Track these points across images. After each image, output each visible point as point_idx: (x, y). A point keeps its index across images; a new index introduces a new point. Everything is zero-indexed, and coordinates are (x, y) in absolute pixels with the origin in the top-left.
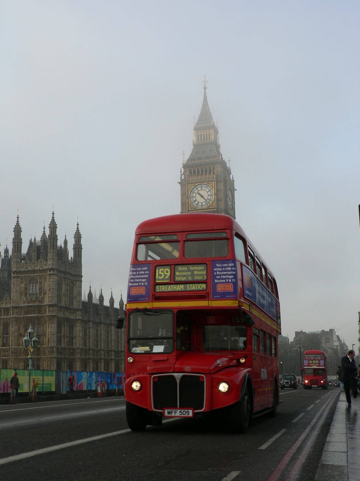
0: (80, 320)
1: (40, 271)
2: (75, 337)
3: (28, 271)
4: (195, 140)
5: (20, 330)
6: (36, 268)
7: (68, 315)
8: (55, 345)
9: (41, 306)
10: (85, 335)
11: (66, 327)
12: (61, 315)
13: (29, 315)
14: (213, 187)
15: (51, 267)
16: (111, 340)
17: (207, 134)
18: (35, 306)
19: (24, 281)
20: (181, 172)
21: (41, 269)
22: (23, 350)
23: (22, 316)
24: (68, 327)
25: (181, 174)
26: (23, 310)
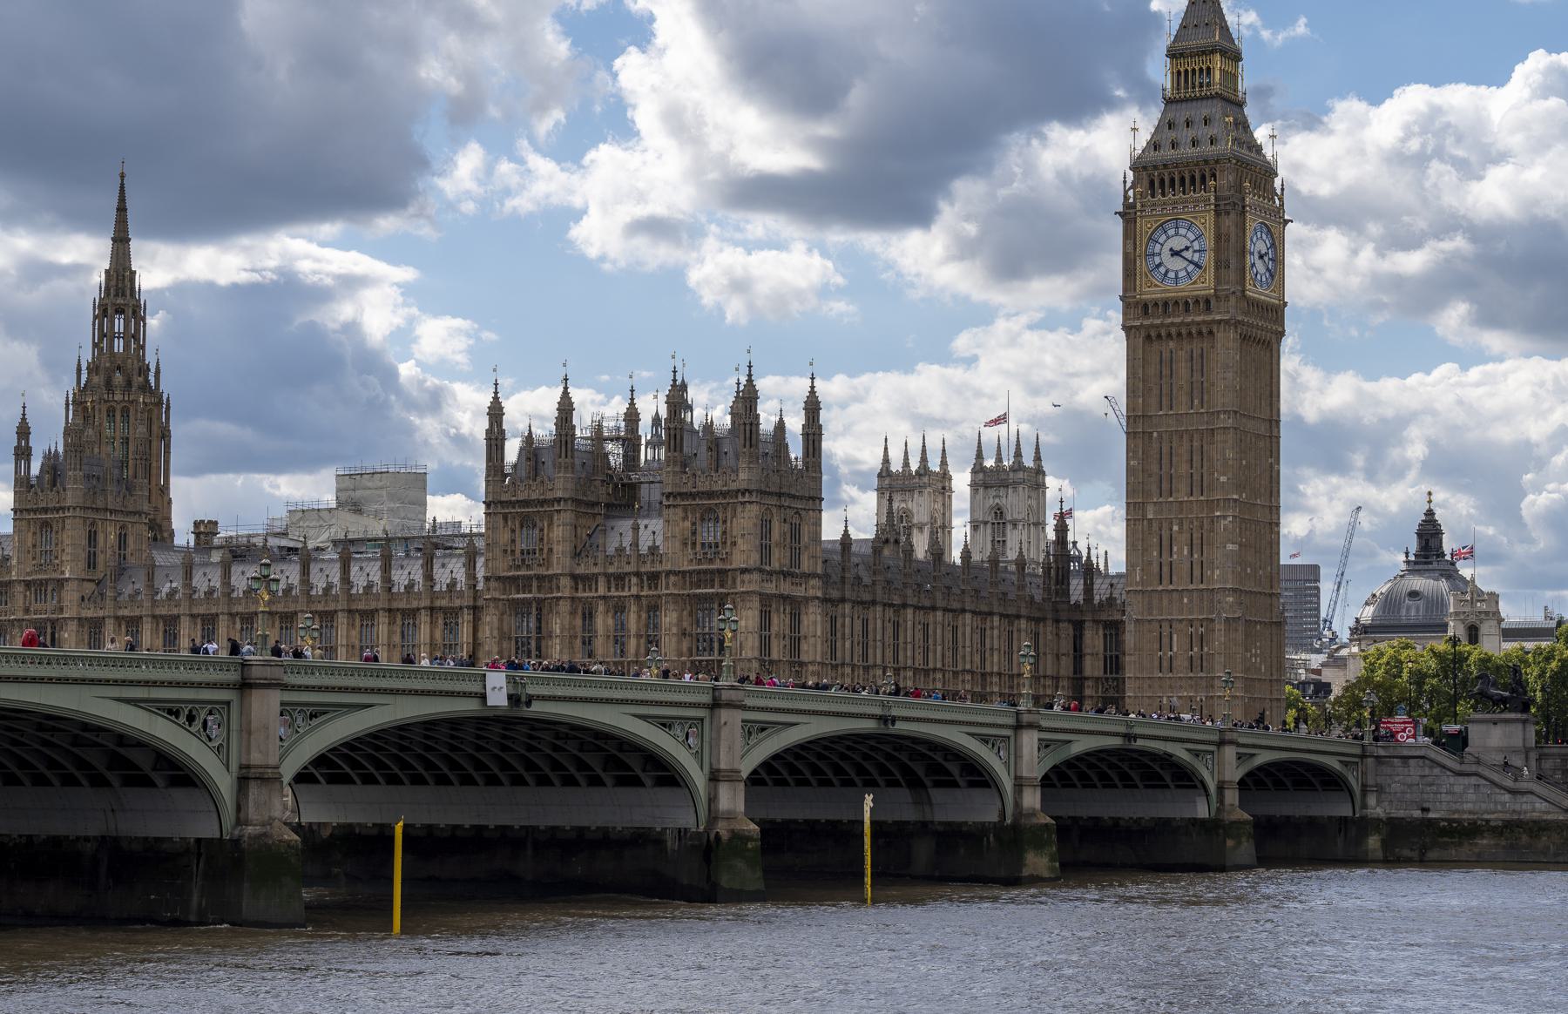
0: (818, 598)
1: (724, 494)
2: (806, 637)
3: (699, 492)
4: (1169, 86)
5: (682, 621)
6: (717, 488)
7: (786, 588)
8: (757, 654)
9: (726, 571)
10: (834, 632)
11: (782, 616)
12: (770, 588)
13: (700, 591)
14: (1205, 227)
15: (744, 486)
16: (905, 643)
17: (1201, 70)
18: (712, 572)
19: (690, 516)
20: (1125, 182)
21: (725, 488)
22: (688, 665)
23: (685, 592)
24: (788, 616)
25: (1125, 186)
26: (688, 579)
